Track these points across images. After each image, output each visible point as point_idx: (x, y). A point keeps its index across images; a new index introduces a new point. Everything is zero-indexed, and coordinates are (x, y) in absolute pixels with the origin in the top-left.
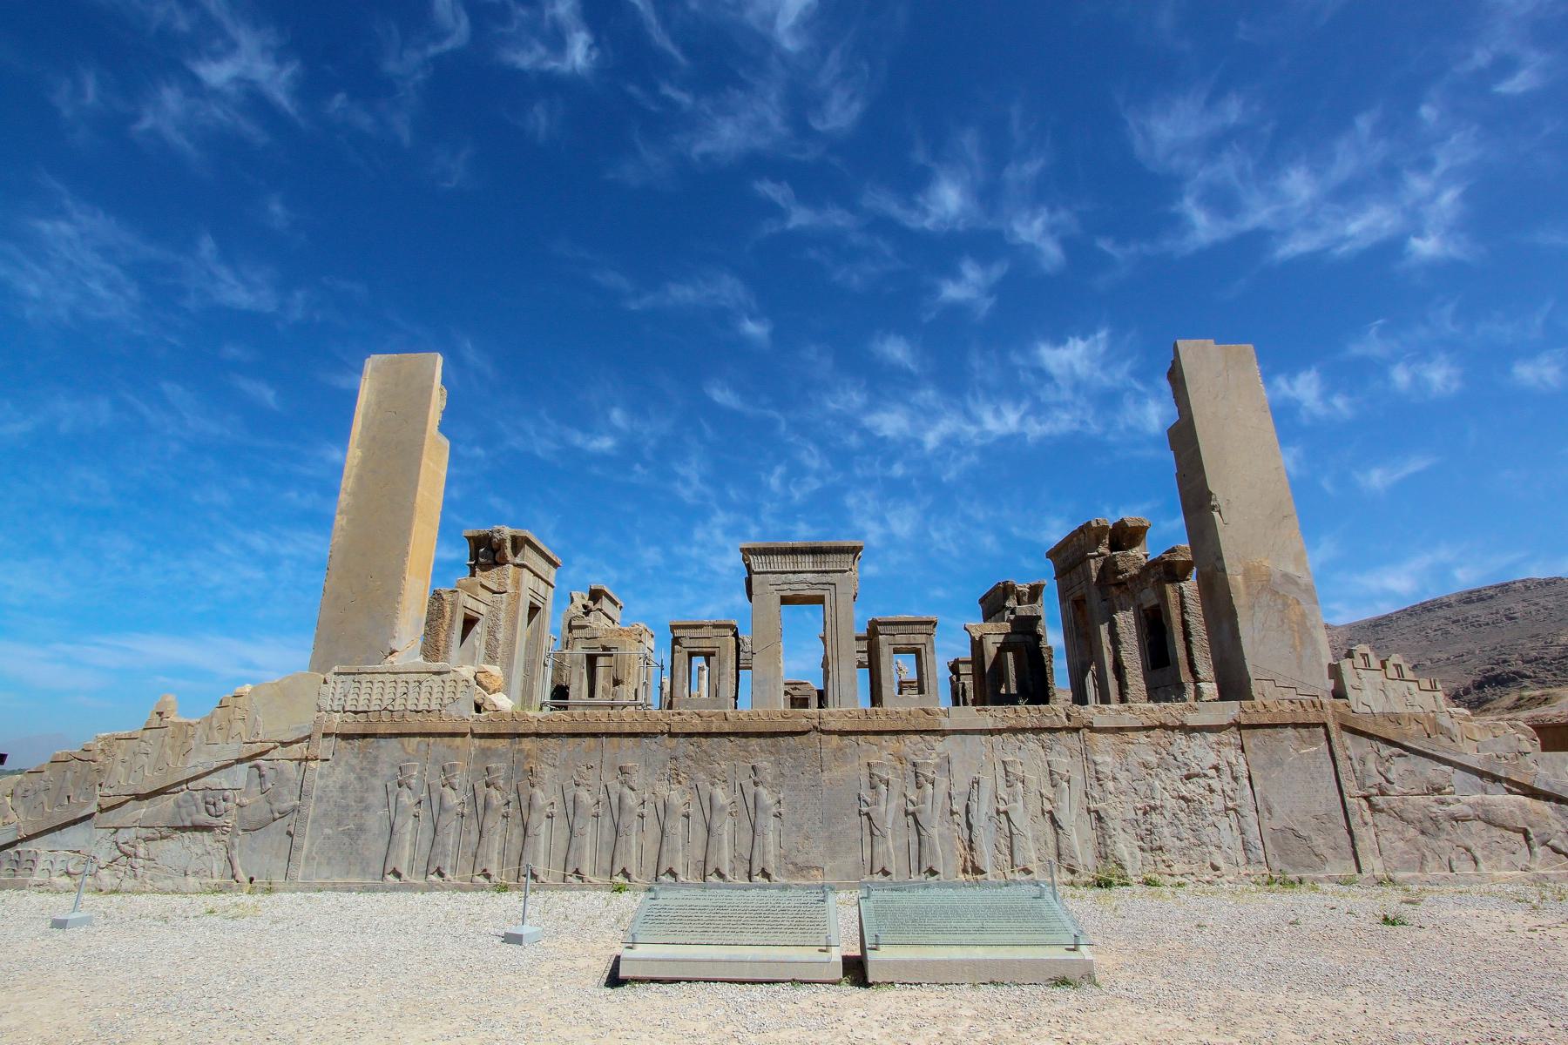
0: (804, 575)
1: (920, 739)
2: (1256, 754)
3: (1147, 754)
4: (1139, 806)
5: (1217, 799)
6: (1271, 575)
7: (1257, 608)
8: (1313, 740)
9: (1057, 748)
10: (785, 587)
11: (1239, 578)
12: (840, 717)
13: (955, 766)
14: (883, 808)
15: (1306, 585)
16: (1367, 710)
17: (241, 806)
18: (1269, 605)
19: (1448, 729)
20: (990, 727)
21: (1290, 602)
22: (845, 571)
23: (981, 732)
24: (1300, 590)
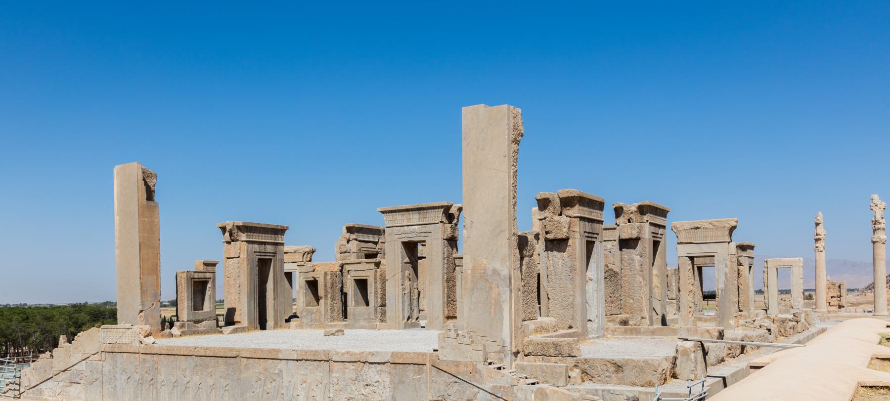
0: (412, 227)
1: (272, 362)
2: (395, 377)
3: (352, 375)
4: (346, 396)
5: (376, 396)
6: (486, 270)
7: (475, 291)
8: (420, 372)
9: (319, 369)
10: (403, 236)
11: (469, 271)
12: (247, 351)
13: (284, 374)
14: (258, 391)
15: (504, 276)
16: (445, 359)
17: (86, 376)
18: (481, 288)
19: (480, 371)
20: (295, 359)
21: (493, 286)
22: (437, 223)
23: (293, 360)
24: (500, 278)
